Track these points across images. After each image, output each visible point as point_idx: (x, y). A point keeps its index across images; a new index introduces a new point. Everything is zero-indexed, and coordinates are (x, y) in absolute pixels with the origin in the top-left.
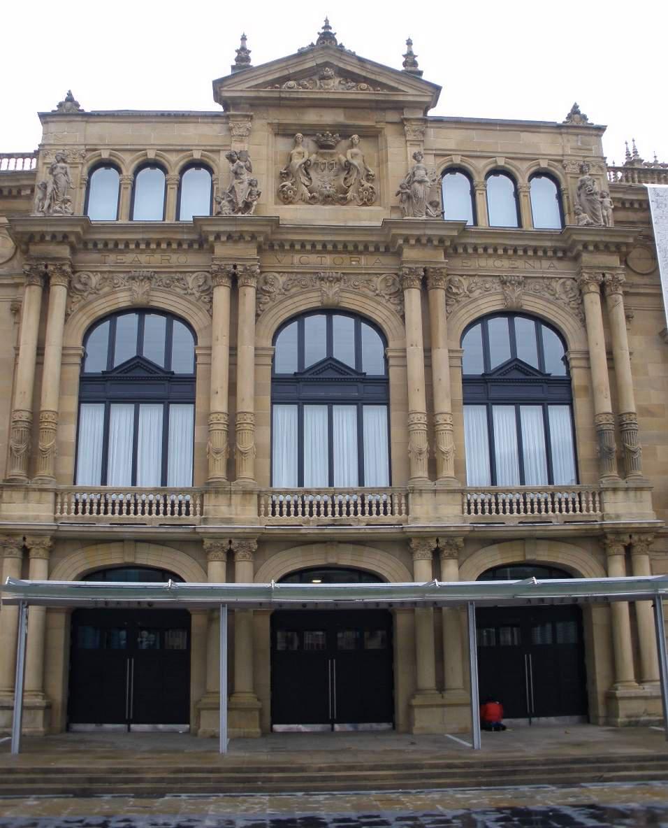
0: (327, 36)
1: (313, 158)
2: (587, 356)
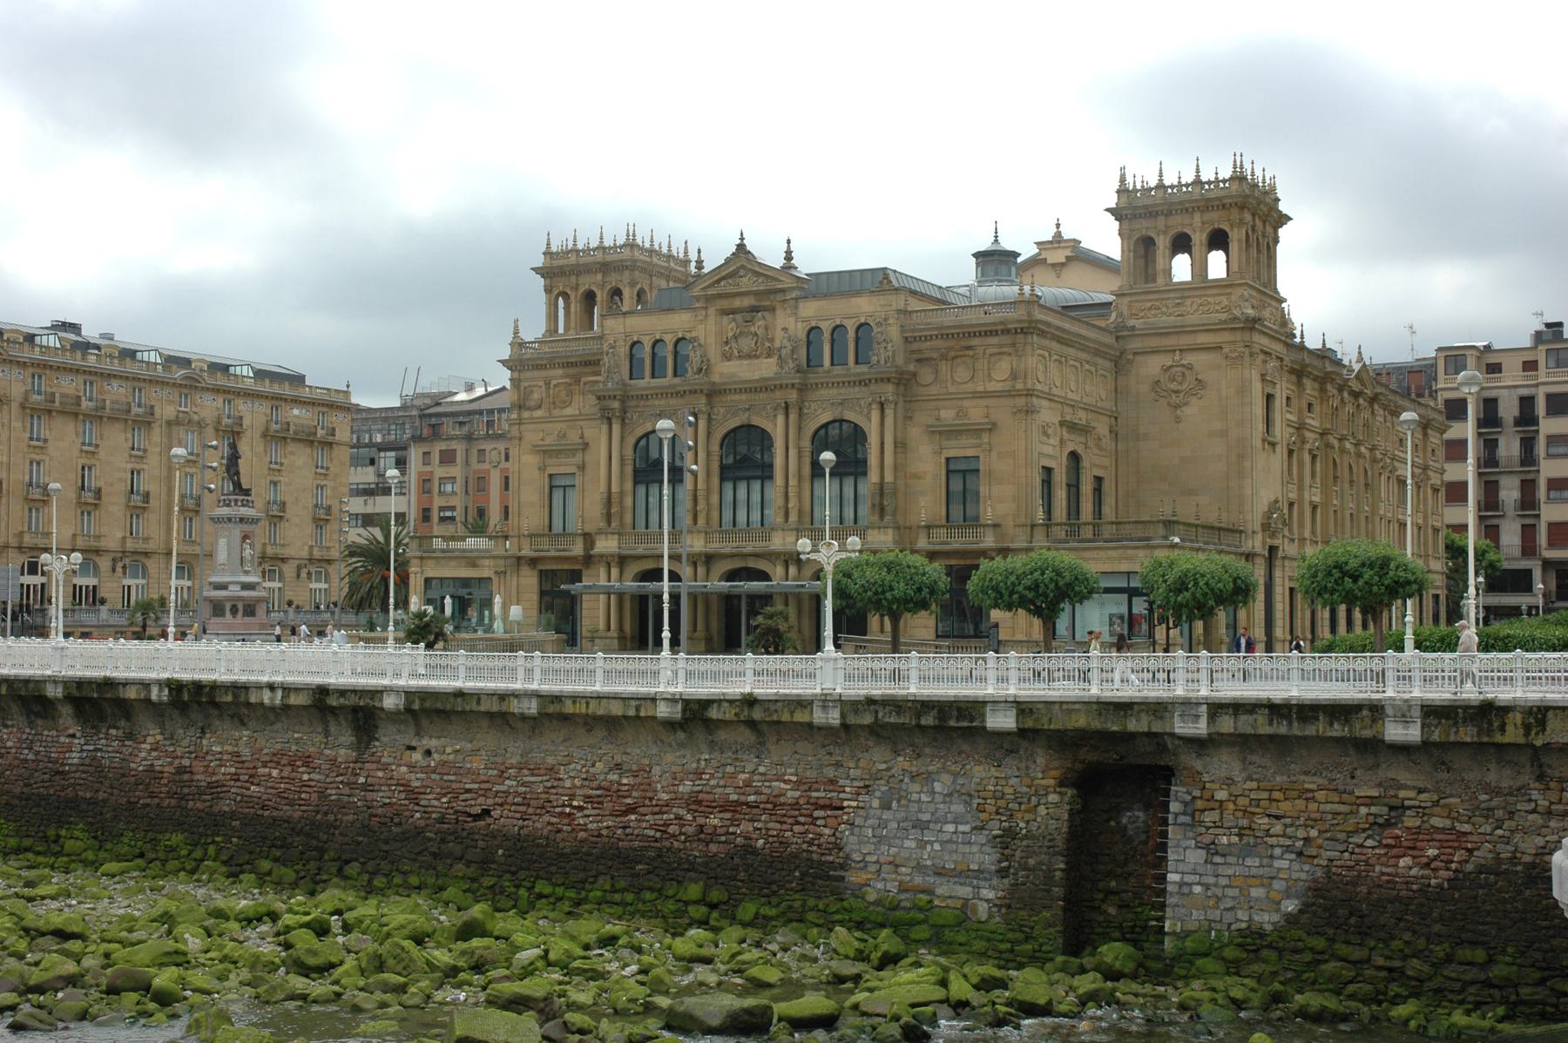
0: (741, 247)
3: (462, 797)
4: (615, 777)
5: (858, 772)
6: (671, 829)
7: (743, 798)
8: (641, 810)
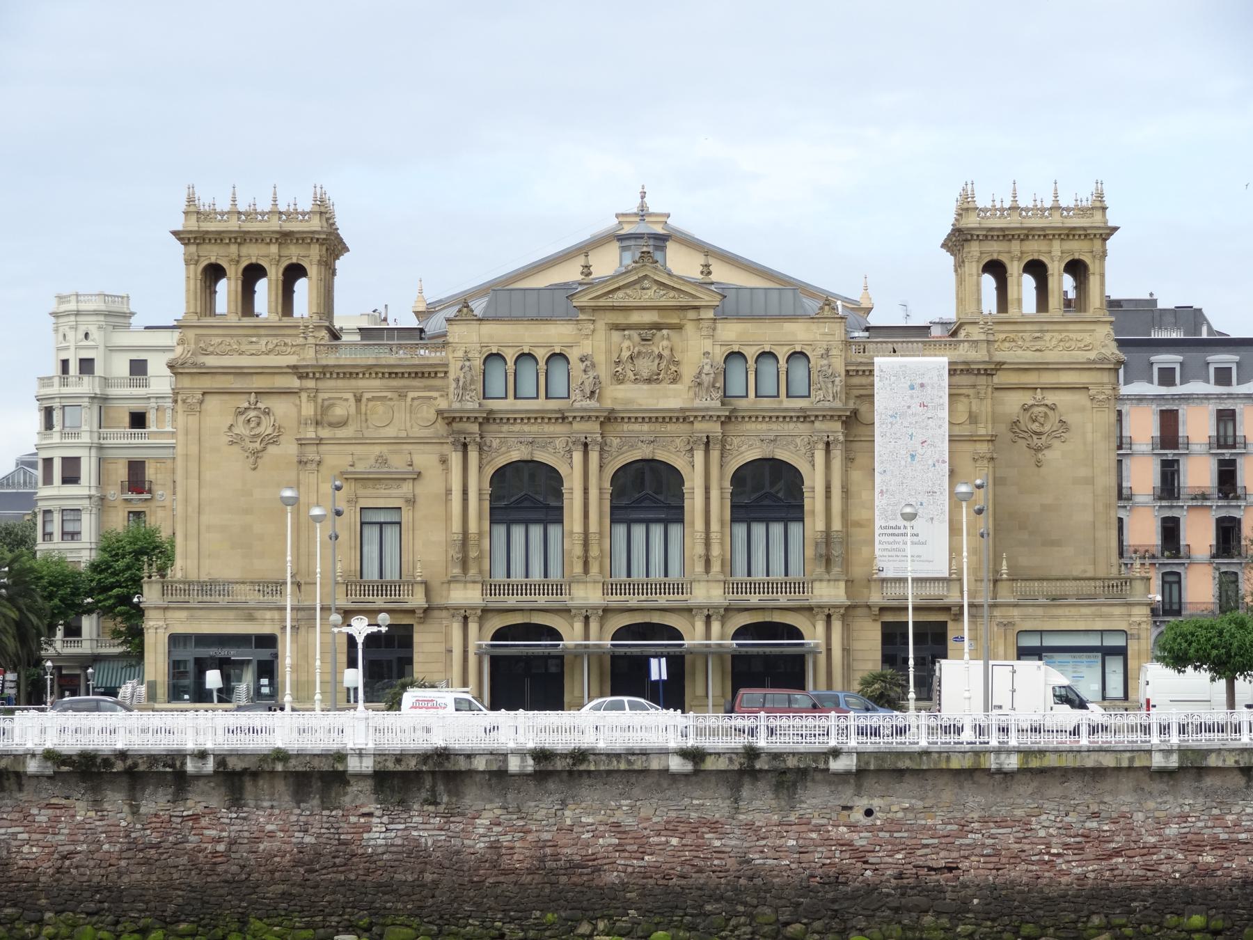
1: (636, 350)
2: (813, 489)
3: (919, 852)
4: (1095, 825)
6: (1163, 868)
7: (1234, 836)
8: (1129, 853)
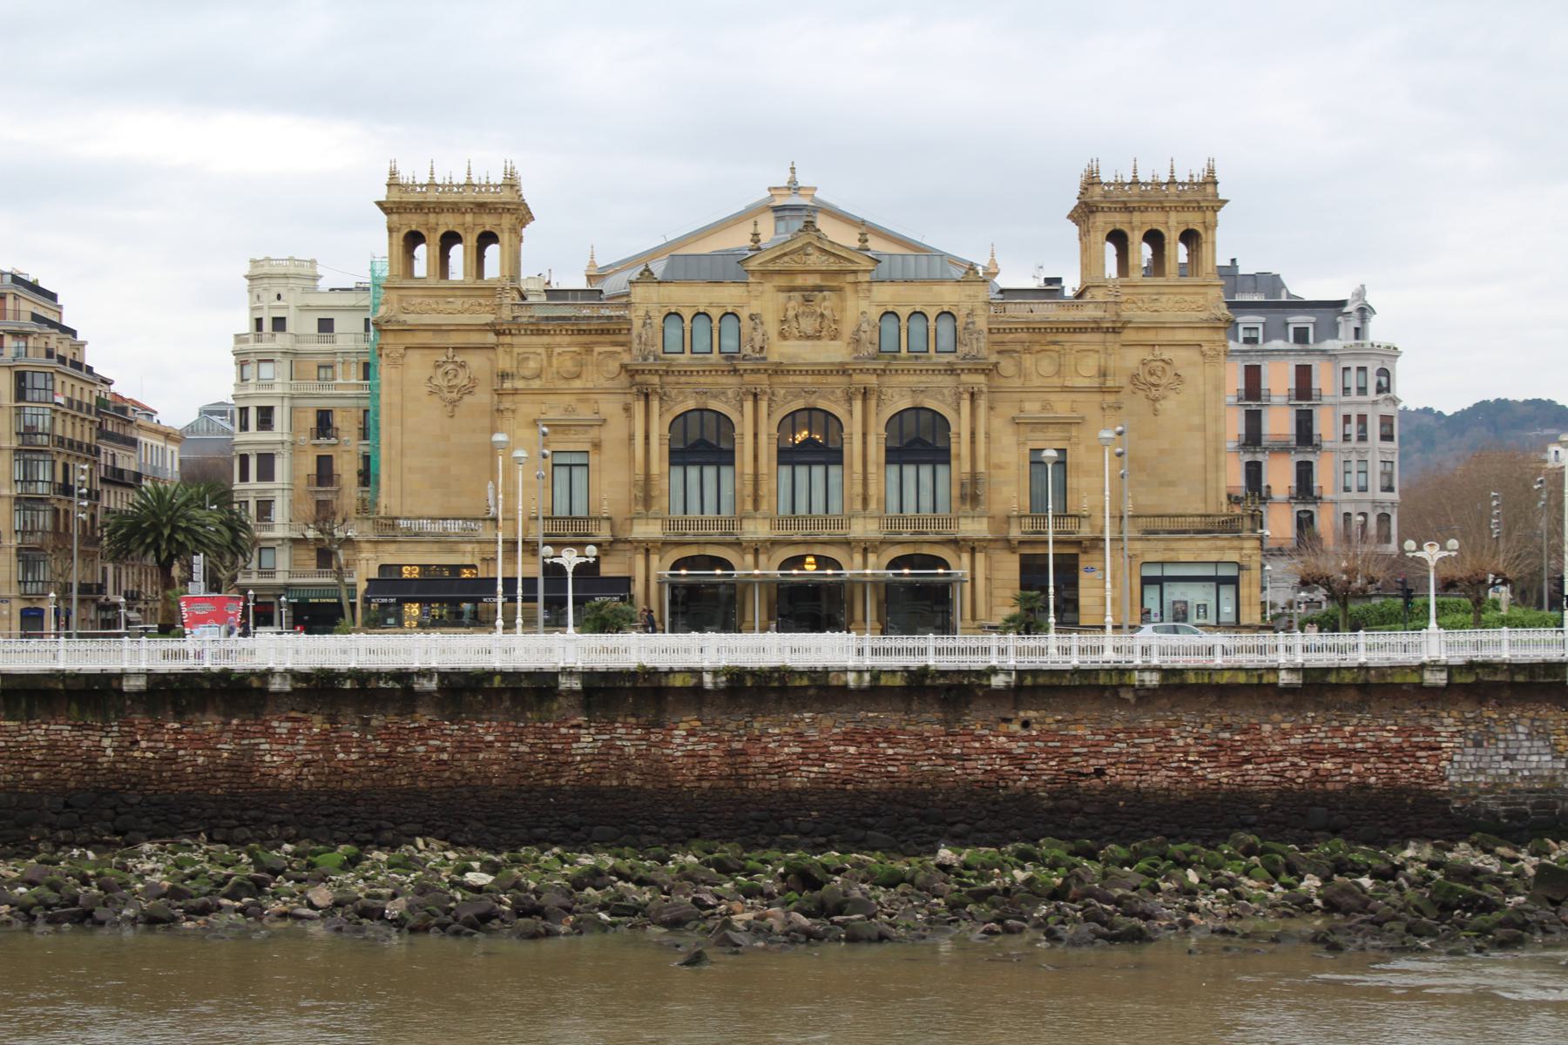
4: (1227, 735)
5: (1451, 721)
6: (1288, 774)
